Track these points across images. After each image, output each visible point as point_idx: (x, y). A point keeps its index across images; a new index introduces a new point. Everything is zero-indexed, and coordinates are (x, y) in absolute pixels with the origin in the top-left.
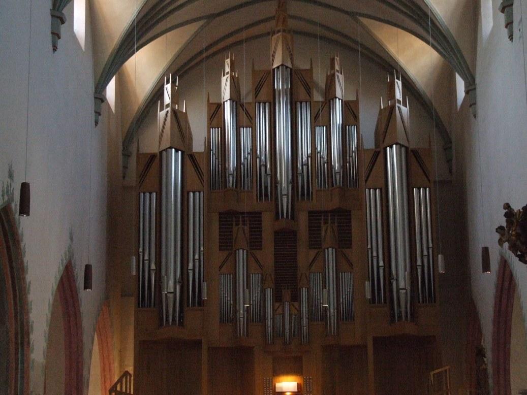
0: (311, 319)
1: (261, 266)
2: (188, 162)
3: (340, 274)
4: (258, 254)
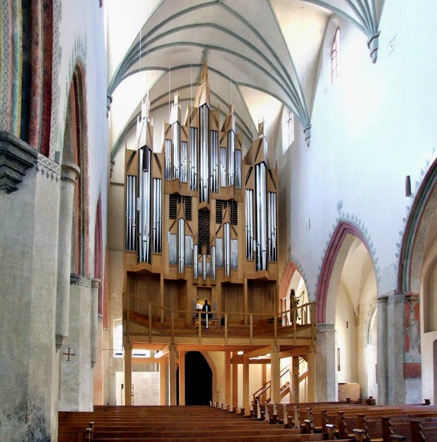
4: (189, 222)
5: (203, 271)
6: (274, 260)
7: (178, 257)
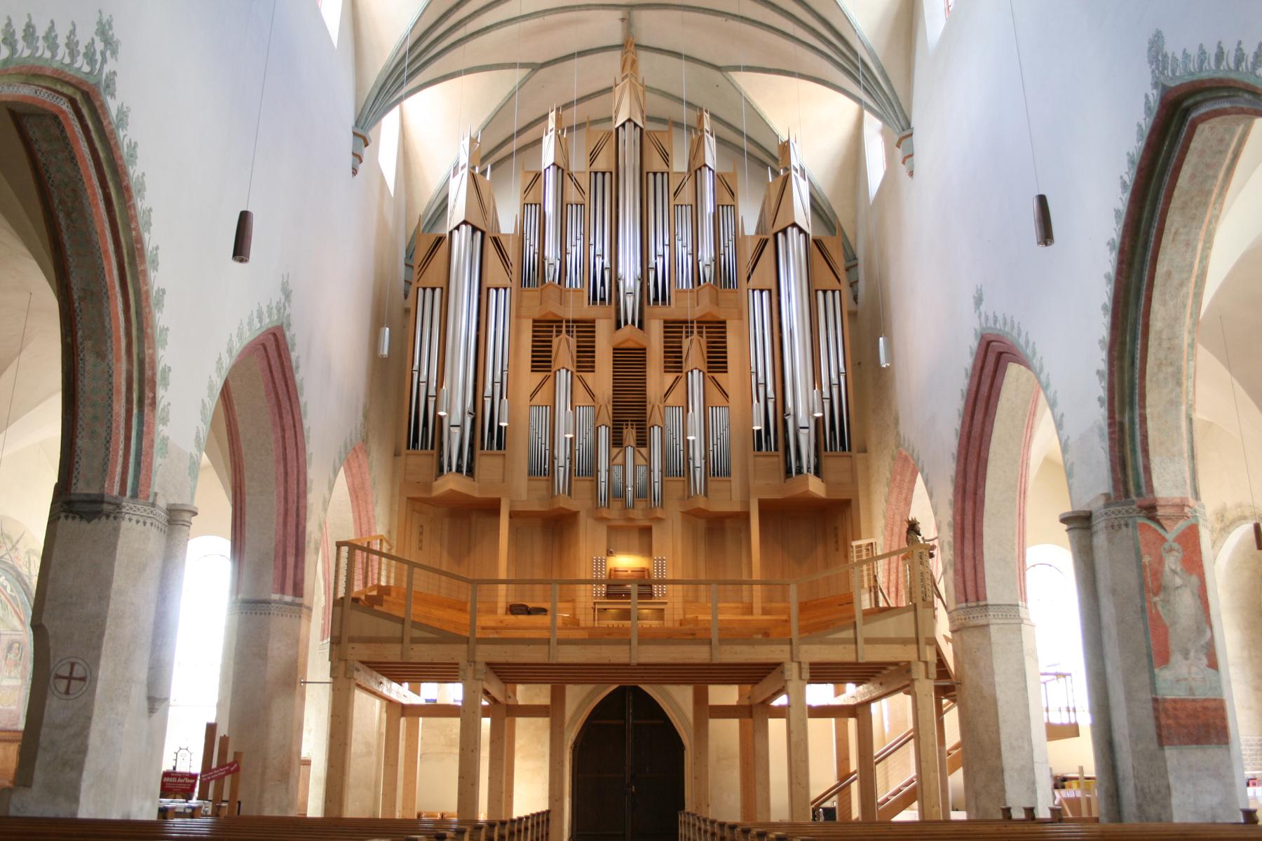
0: (666, 471)
1: (592, 395)
2: (490, 246)
3: (710, 408)
4: (588, 377)
5: (625, 487)
6: (844, 449)
7: (553, 458)
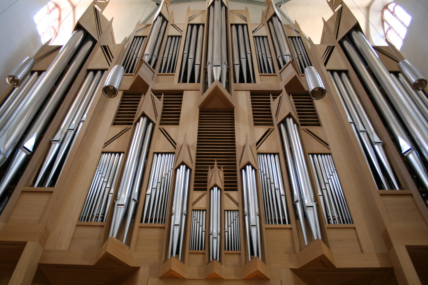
4: (171, 130)
5: (208, 234)
